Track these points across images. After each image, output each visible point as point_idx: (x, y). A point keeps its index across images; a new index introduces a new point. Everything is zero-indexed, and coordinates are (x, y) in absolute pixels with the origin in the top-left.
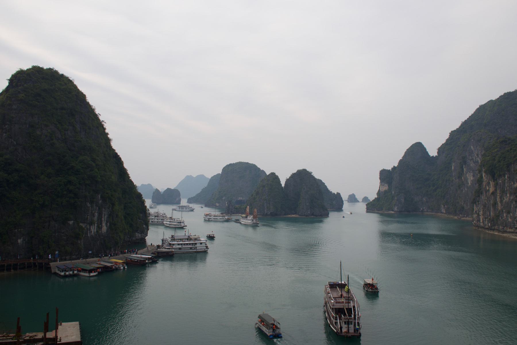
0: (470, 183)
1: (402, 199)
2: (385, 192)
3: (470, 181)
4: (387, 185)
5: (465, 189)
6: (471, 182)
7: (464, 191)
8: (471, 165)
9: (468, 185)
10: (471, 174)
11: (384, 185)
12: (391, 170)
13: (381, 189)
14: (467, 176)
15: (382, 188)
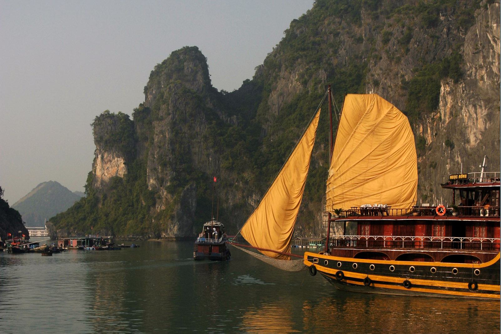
0: (472, 139)
1: (190, 200)
2: (116, 180)
3: (474, 133)
4: (122, 161)
5: (452, 159)
6: (480, 137)
7: (448, 166)
8: (480, 84)
9: (467, 146)
10: (479, 111)
11: (111, 161)
12: (131, 118)
13: (99, 173)
14: (462, 119)
15: (103, 168)
